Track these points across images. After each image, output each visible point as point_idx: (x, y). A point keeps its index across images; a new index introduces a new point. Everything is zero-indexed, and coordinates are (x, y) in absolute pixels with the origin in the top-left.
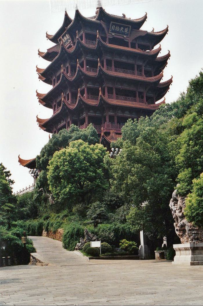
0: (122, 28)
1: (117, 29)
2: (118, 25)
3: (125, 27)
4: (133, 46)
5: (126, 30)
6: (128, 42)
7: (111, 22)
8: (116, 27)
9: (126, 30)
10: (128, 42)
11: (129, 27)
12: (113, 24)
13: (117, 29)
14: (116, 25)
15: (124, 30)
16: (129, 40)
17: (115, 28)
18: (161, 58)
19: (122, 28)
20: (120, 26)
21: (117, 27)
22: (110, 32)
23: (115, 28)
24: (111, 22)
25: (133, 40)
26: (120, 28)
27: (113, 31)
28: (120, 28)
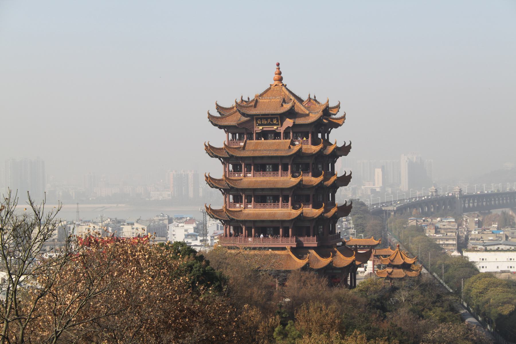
2: (264, 118)
6: (280, 133)
7: (255, 117)
8: (261, 120)
9: (275, 122)
10: (280, 133)
15: (272, 121)
16: (282, 130)
17: (261, 122)
19: (269, 121)
20: (267, 119)
21: (263, 120)
22: (257, 126)
23: (261, 122)
24: (255, 117)
25: (285, 131)
27: (260, 125)
28: (267, 120)
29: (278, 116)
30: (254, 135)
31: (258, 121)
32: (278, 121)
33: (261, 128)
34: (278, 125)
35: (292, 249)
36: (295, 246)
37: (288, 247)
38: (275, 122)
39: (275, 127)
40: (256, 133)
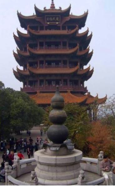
0: (54, 18)
1: (51, 19)
3: (56, 17)
4: (64, 28)
9: (57, 19)
10: (60, 27)
12: (47, 17)
13: (51, 19)
14: (49, 17)
15: (55, 19)
17: (49, 19)
18: (89, 36)
19: (54, 18)
20: (52, 17)
24: (46, 16)
26: (52, 18)
27: (48, 21)
28: (52, 18)
29: (60, 16)
30: (44, 27)
31: (47, 19)
32: (59, 19)
33: (48, 23)
35: (71, 92)
36: (72, 90)
37: (69, 91)
38: (57, 19)
39: (57, 23)
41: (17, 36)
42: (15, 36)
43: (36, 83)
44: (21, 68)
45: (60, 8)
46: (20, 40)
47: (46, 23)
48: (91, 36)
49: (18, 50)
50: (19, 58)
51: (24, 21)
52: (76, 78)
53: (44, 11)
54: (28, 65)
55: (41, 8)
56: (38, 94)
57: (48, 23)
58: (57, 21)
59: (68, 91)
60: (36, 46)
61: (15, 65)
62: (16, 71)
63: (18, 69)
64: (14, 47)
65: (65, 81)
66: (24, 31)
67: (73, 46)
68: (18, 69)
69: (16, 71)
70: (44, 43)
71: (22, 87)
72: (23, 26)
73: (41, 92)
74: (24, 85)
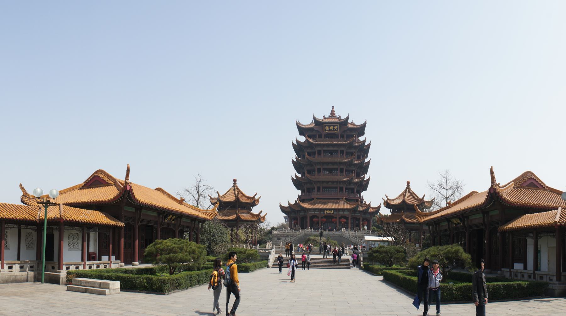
3: (334, 126)
5: (336, 128)
7: (324, 125)
10: (338, 135)
11: (337, 126)
29: (339, 125)
32: (337, 128)
33: (327, 132)
34: (337, 130)
39: (336, 132)
40: (324, 135)
41: (295, 143)
42: (293, 144)
43: (313, 190)
44: (300, 176)
45: (340, 116)
46: (298, 148)
47: (324, 131)
48: (369, 145)
49: (296, 158)
50: (297, 165)
51: (302, 130)
52: (352, 186)
53: (323, 120)
54: (306, 172)
55: (320, 117)
56: (315, 199)
57: (327, 132)
58: (336, 130)
59: (343, 197)
60: (314, 153)
61: (293, 173)
62: (295, 178)
63: (296, 176)
64: (293, 155)
65: (341, 189)
66: (302, 139)
67: (350, 154)
68: (296, 176)
69: (295, 178)
70: (322, 152)
71: (300, 194)
72: (301, 133)
73: (317, 199)
74: (302, 192)
